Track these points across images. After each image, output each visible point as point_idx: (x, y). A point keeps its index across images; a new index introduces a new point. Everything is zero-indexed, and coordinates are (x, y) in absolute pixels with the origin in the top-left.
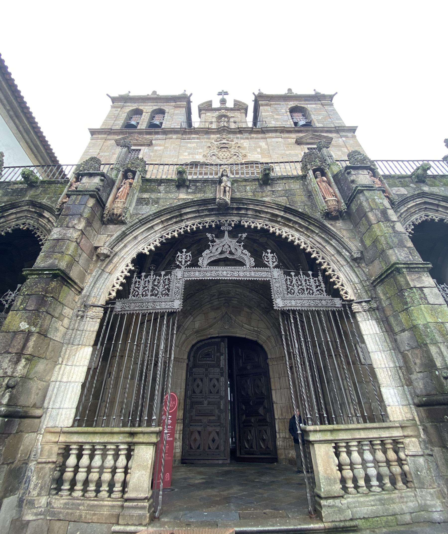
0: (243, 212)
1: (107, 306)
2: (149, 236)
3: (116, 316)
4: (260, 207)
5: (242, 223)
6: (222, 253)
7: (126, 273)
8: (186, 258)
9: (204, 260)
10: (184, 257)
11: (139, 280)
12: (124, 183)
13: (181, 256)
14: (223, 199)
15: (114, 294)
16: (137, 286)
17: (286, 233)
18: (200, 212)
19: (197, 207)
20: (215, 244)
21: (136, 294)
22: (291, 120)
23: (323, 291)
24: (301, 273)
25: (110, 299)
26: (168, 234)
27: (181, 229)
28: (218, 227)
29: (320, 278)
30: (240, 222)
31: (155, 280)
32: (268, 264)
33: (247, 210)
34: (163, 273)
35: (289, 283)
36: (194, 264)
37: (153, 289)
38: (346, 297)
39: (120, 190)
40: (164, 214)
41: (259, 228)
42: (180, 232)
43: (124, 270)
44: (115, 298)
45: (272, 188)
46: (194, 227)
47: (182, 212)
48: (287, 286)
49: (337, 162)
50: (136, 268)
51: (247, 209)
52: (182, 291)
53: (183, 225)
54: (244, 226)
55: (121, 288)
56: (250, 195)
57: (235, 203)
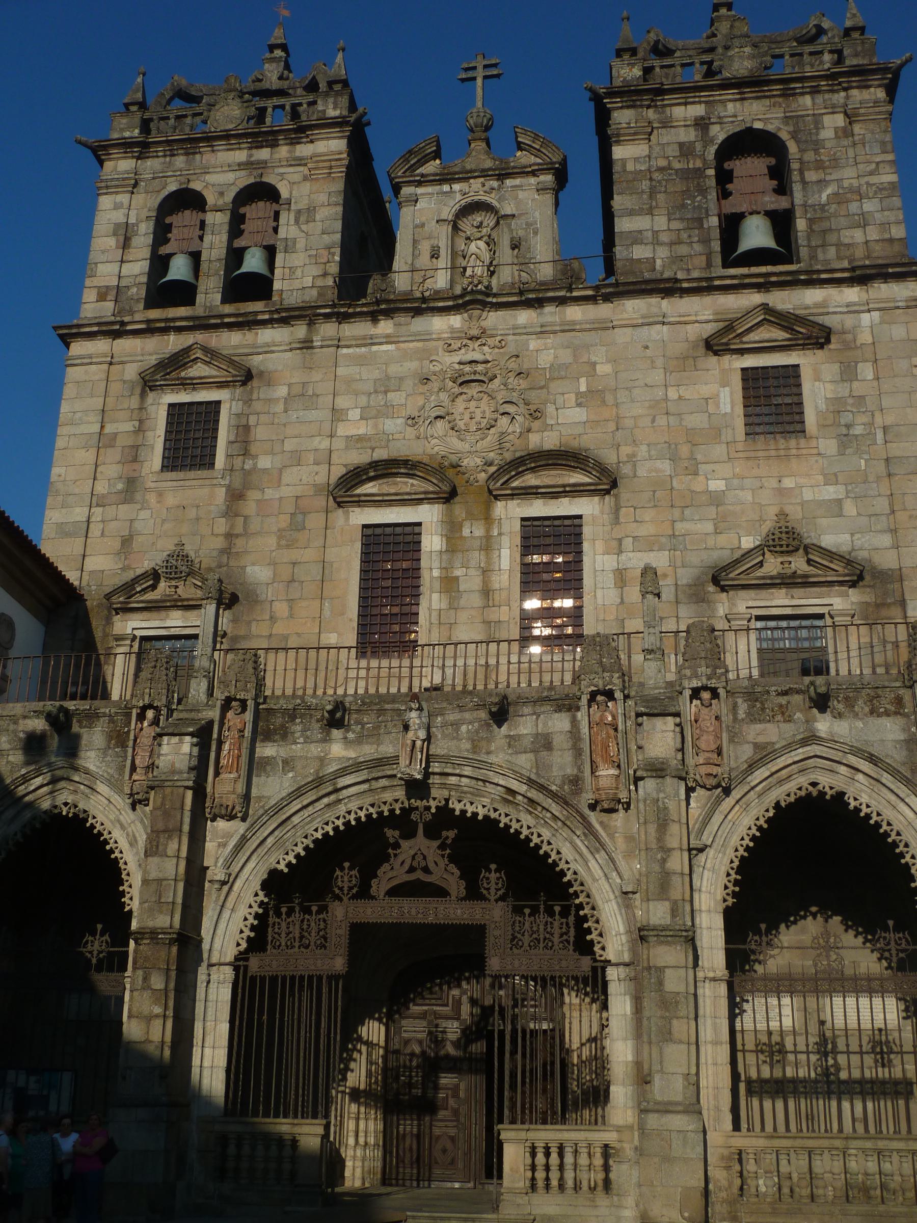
0: (453, 780)
1: (238, 963)
2: (285, 837)
3: (253, 978)
5: (451, 806)
6: (412, 870)
7: (256, 908)
8: (350, 881)
9: (379, 886)
10: (346, 879)
11: (279, 920)
13: (342, 877)
15: (244, 945)
16: (276, 930)
17: (529, 827)
20: (399, 851)
21: (278, 944)
23: (568, 942)
24: (542, 910)
25: (241, 953)
26: (316, 830)
27: (338, 818)
28: (406, 812)
29: (572, 919)
30: (447, 800)
31: (302, 921)
32: (487, 895)
34: (314, 909)
35: (517, 929)
36: (363, 892)
37: (302, 937)
38: (601, 956)
41: (480, 817)
42: (338, 827)
43: (253, 904)
44: (247, 951)
46: (362, 814)
48: (512, 935)
50: (270, 899)
51: (461, 776)
52: (345, 941)
53: (342, 809)
54: (454, 810)
55: (252, 934)
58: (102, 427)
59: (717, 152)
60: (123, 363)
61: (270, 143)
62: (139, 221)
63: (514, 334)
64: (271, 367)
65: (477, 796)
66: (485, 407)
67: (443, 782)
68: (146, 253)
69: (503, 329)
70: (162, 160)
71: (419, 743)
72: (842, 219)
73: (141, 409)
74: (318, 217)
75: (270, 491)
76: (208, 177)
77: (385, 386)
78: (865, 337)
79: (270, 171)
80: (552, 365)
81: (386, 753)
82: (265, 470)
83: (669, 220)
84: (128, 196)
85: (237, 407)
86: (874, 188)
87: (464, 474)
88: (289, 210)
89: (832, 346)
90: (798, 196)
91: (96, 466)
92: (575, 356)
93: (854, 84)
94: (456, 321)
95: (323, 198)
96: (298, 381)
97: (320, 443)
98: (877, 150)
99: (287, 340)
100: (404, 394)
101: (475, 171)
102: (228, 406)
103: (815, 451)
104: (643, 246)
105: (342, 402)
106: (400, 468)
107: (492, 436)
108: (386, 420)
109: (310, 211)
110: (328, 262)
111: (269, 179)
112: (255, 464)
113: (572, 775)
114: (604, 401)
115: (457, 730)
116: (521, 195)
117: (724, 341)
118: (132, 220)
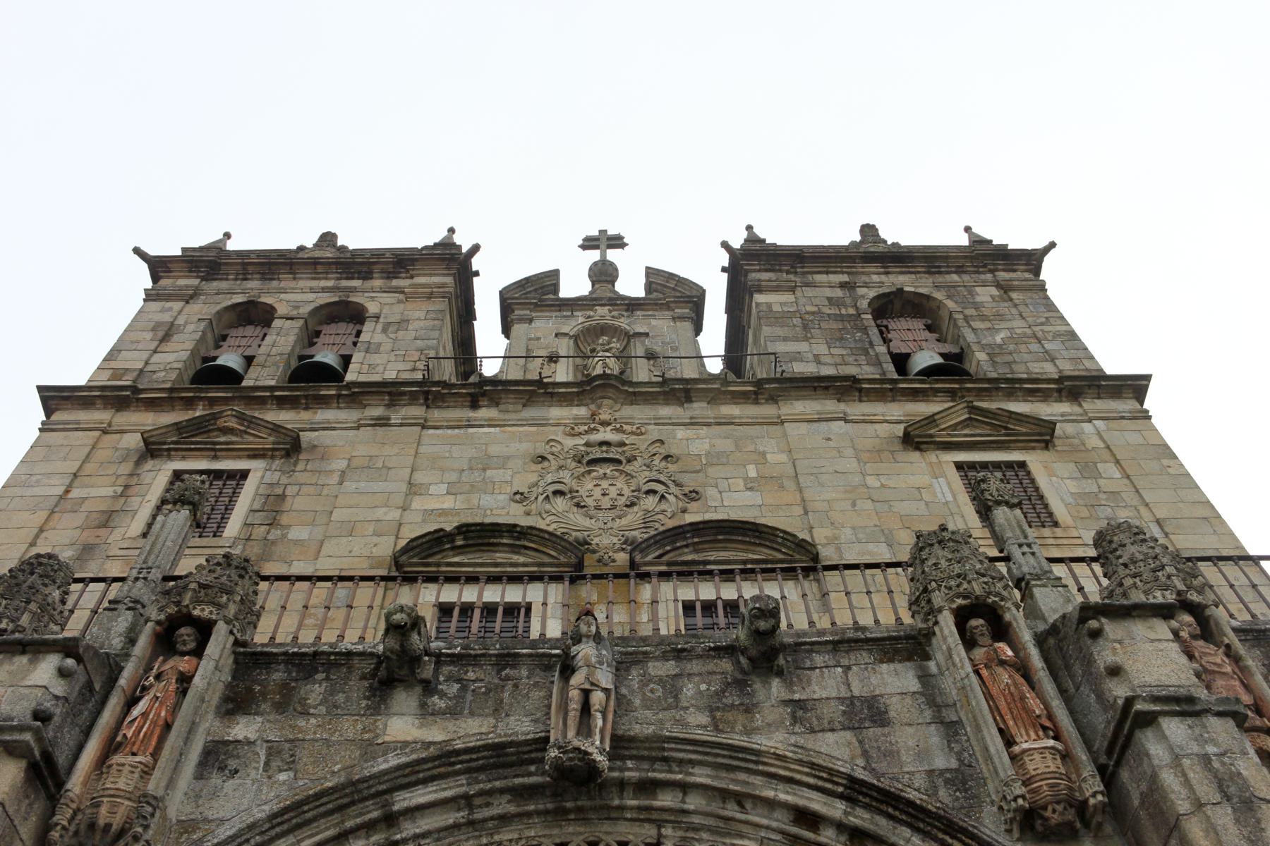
0: (666, 800)
4: (742, 776)
12: (158, 677)
14: (577, 749)
18: (477, 801)
19: (463, 780)
22: (882, 349)
33: (685, 794)
39: (137, 711)
40: (315, 819)
45: (789, 685)
47: (396, 808)
49: (1059, 570)
51: (685, 788)
56: (697, 723)
57: (631, 758)
58: (67, 492)
59: (870, 304)
60: (123, 432)
61: (363, 275)
62: (186, 323)
63: (656, 424)
64: (328, 442)
65: (728, 835)
66: (620, 488)
67: (646, 803)
68: (190, 345)
69: (642, 419)
70: (232, 282)
71: (597, 698)
72: (1026, 355)
73: (131, 475)
74: (410, 327)
75: (302, 564)
76: (282, 296)
77: (484, 463)
78: (1094, 442)
79: (361, 294)
80: (708, 454)
81: (516, 734)
82: (296, 542)
83: (829, 348)
84: (181, 304)
85: (273, 477)
86: (1051, 334)
87: (594, 552)
88: (376, 322)
89: (1059, 448)
90: (970, 336)
91: (41, 530)
92: (737, 446)
93: (1000, 267)
94: (582, 411)
95: (422, 315)
96: (364, 454)
97: (385, 514)
98: (1042, 309)
99: (355, 419)
100: (510, 472)
101: (601, 299)
102: (259, 474)
103: (1079, 541)
104: (804, 364)
105: (419, 477)
106: (502, 537)
107: (633, 517)
108: (483, 496)
109: (403, 323)
110: (419, 360)
111: (354, 298)
112: (284, 536)
113: (947, 770)
114: (782, 487)
115: (675, 694)
116: (654, 322)
117: (932, 432)
118: (181, 321)
